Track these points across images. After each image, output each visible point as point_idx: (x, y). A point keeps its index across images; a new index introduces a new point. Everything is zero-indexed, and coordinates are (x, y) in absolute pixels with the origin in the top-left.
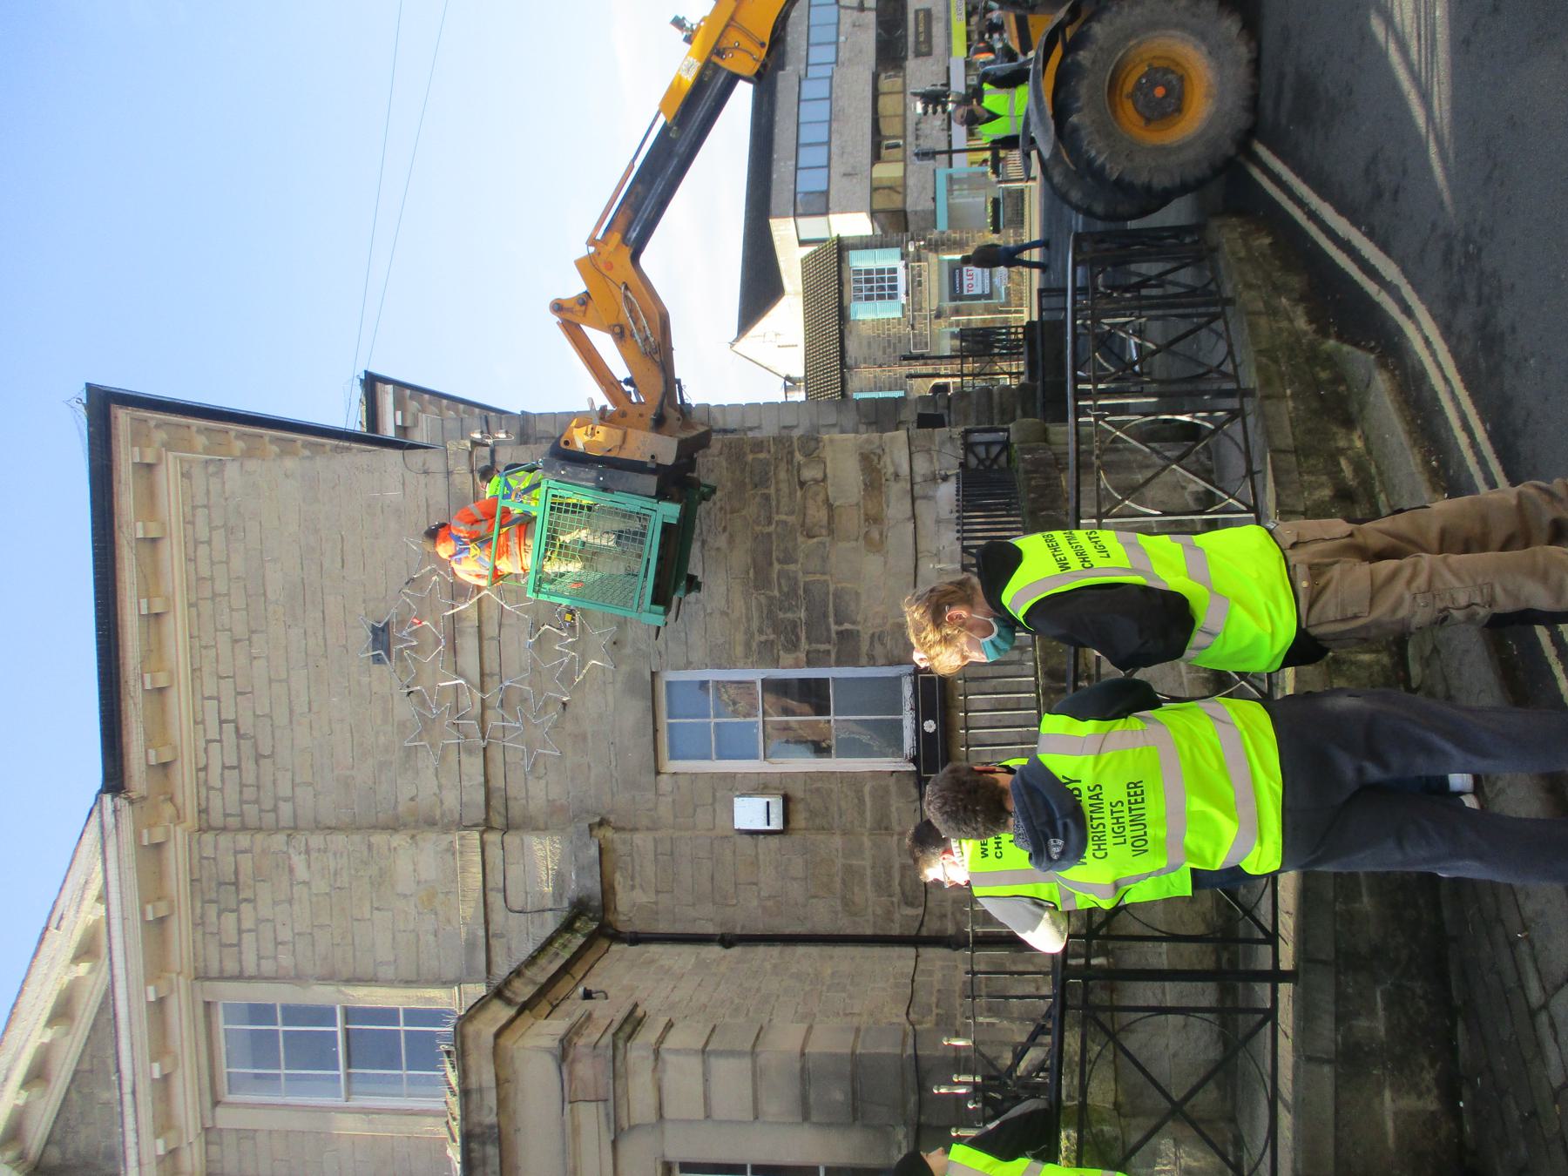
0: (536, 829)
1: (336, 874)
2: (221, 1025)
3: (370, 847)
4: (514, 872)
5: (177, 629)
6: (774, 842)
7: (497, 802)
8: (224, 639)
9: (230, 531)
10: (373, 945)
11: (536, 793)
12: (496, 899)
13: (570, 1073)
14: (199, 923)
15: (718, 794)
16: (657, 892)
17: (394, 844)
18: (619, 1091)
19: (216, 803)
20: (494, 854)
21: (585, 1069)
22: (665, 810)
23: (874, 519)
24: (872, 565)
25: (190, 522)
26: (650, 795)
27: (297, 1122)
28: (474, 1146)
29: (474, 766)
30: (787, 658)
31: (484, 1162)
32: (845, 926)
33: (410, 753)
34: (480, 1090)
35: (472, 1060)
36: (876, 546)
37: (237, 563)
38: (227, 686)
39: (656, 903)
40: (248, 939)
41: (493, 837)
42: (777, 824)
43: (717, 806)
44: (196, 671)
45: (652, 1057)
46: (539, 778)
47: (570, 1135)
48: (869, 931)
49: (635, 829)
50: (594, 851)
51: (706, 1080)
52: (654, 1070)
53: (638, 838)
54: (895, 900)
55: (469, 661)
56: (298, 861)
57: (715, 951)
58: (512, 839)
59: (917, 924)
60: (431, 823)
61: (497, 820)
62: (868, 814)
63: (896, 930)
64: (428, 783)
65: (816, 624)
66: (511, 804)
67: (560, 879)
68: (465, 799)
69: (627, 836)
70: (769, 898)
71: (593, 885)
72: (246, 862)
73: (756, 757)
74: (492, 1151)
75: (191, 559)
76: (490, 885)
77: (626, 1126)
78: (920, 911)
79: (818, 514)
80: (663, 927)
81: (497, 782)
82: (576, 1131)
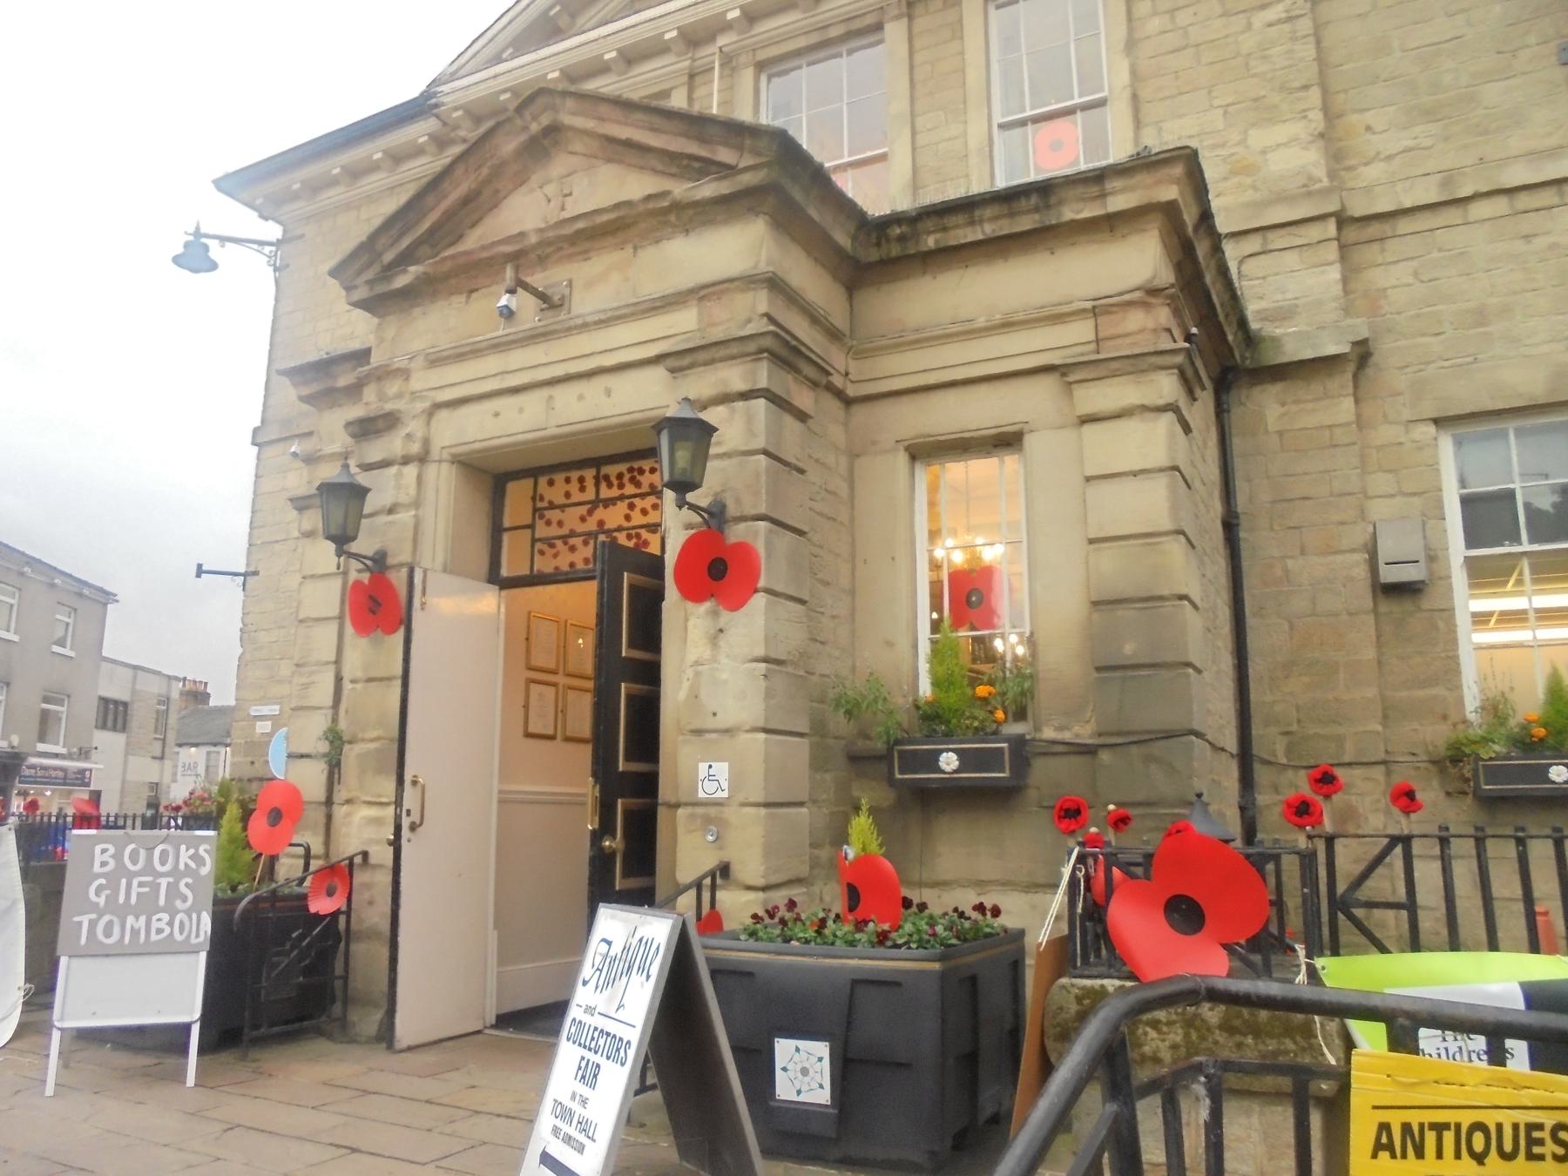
0: (1345, 281)
1: (1265, 57)
3: (1306, 87)
4: (1291, 259)
6: (1361, 572)
7: (1374, 229)
10: (1180, 116)
11: (1395, 273)
12: (1253, 244)
13: (1130, 304)
15: (1415, 500)
16: (1280, 433)
17: (1311, 115)
18: (1115, 365)
20: (1313, 233)
22: (1386, 433)
26: (1407, 414)
27: (974, 77)
28: (1034, 200)
31: (1012, 215)
32: (1255, 667)
34: (1103, 196)
35: (1143, 178)
39: (1267, 432)
41: (1331, 228)
42: (1389, 575)
43: (1398, 500)
45: (1161, 402)
46: (1416, 274)
48: (1254, 696)
49: (1357, 401)
50: (1331, 349)
51: (1135, 474)
52: (1145, 408)
53: (1348, 403)
54: (1295, 727)
57: (1218, 508)
58: (1332, 251)
59: (1265, 756)
60: (1337, 156)
61: (1351, 234)
62: (1405, 694)
63: (1257, 730)
66: (1376, 247)
67: (1284, 314)
68: (1377, 189)
69: (1350, 390)
70: (1286, 571)
71: (1295, 351)
73: (1471, 542)
74: (1025, 223)
76: (1271, 235)
77: (1071, 378)
78: (1284, 761)
80: (1237, 444)
81: (1404, 226)
82: (1057, 319)
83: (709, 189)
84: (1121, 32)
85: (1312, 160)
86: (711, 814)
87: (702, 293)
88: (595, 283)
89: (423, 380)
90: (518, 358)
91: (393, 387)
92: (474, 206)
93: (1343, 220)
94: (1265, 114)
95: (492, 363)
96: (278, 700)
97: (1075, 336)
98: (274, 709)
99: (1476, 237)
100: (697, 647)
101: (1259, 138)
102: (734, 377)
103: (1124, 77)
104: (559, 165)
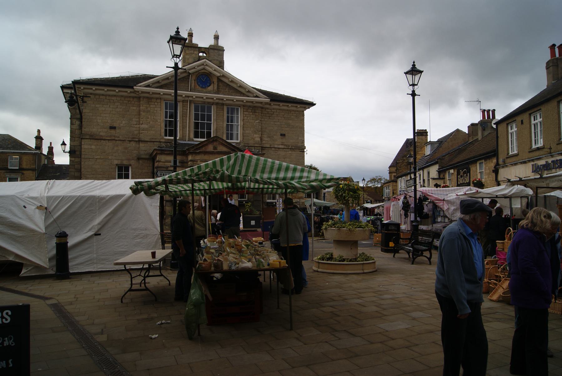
5: (285, 108)
8: (283, 114)
14: (250, 106)
25: (297, 111)
29: (268, 146)
33: (269, 137)
37: (292, 117)
38: (278, 113)
40: (248, 113)
44: (280, 109)
55: (281, 147)
56: (257, 121)
60: (261, 139)
64: (266, 139)
72: (257, 114)
75: (293, 111)
84: (242, 118)
85: (259, 139)
93: (262, 147)
104: (215, 143)
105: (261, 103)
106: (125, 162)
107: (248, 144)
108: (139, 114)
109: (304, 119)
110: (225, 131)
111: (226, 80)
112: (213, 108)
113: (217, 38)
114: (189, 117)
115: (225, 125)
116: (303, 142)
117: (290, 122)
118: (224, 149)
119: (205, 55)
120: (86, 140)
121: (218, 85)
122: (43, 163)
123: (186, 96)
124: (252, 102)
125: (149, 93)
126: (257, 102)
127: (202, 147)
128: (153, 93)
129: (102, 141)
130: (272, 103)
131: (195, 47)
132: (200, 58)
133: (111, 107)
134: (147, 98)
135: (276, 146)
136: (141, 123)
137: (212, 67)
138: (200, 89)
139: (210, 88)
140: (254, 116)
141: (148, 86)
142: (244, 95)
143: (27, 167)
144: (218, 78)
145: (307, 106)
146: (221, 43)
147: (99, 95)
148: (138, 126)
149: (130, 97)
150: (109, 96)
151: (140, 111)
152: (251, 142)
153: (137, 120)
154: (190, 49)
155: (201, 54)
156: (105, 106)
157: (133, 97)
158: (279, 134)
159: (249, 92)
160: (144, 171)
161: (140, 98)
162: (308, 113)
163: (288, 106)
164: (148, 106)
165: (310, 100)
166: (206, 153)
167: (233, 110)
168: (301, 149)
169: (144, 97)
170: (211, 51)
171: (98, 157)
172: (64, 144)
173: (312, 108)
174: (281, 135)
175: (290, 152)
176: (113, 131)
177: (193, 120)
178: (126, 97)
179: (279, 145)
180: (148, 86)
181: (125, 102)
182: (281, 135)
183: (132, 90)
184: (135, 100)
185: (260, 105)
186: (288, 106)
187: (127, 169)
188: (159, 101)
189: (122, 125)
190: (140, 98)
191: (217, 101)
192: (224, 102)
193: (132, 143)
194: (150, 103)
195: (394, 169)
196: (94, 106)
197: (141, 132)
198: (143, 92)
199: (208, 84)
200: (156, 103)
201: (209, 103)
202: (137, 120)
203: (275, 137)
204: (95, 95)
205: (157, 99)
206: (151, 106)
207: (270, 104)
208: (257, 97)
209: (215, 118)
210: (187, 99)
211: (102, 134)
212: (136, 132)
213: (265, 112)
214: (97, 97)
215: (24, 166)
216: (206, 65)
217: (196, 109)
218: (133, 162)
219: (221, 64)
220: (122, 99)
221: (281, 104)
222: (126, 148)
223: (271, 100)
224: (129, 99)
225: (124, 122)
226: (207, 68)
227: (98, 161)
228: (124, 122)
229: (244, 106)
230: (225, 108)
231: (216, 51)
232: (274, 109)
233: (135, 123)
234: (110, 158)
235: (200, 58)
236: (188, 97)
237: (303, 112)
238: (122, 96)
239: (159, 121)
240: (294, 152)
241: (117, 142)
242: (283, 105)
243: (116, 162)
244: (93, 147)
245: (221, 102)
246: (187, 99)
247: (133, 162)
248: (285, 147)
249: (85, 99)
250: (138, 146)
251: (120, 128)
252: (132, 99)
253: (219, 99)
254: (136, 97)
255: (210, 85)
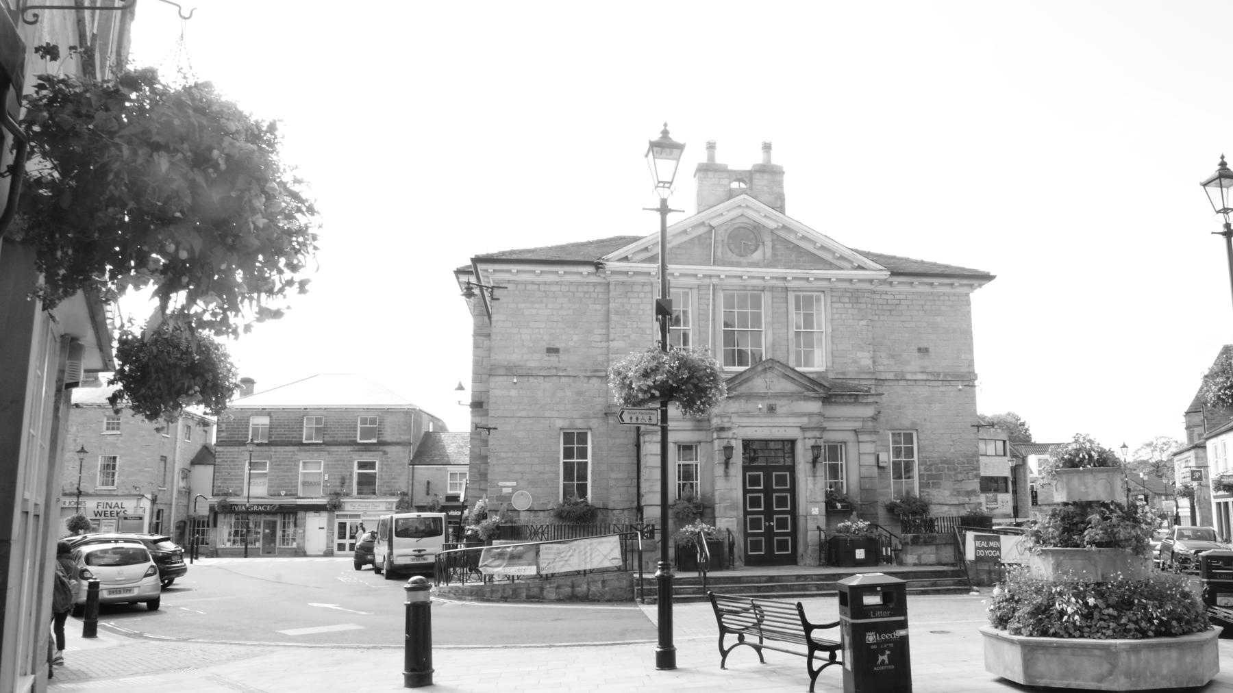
2: (815, 294)
5: (926, 289)
8: (922, 302)
9: (952, 306)
14: (846, 291)
19: (877, 296)
21: (870, 424)
23: (959, 493)
24: (947, 493)
25: (954, 294)
29: (891, 376)
30: (922, 468)
33: (892, 356)
36: (951, 495)
47: (855, 419)
56: (864, 322)
60: (874, 362)
64: (886, 362)
65: (930, 477)
72: (863, 306)
75: (944, 294)
79: (960, 477)
83: (812, 394)
84: (829, 317)
85: (870, 362)
86: (815, 518)
87: (810, 415)
88: (783, 406)
89: (735, 419)
90: (764, 420)
91: (726, 420)
92: (747, 380)
94: (862, 349)
95: (757, 420)
96: (516, 480)
97: (858, 425)
98: (514, 484)
99: (899, 388)
100: (810, 486)
101: (860, 354)
102: (817, 434)
103: (830, 330)
104: (769, 375)
105: (871, 281)
106: (579, 424)
107: (843, 373)
108: (608, 321)
109: (969, 312)
110: (793, 348)
111: (792, 238)
112: (766, 298)
113: (767, 147)
114: (714, 320)
115: (792, 334)
116: (971, 363)
117: (938, 319)
118: (790, 387)
119: (743, 185)
120: (498, 379)
121: (773, 247)
122: (424, 430)
123: (705, 276)
124: (851, 281)
125: (626, 273)
126: (860, 281)
127: (740, 384)
128: (636, 273)
129: (531, 379)
130: (896, 279)
131: (720, 170)
132: (731, 195)
133: (550, 306)
134: (623, 283)
135: (909, 377)
136: (611, 337)
137: (759, 212)
138: (735, 258)
139: (757, 256)
140: (855, 311)
141: (626, 259)
142: (831, 266)
143: (394, 440)
144: (772, 231)
145: (976, 283)
146: (775, 160)
147: (525, 283)
148: (604, 344)
149: (588, 284)
150: (545, 283)
151: (608, 312)
152: (851, 371)
153: (604, 331)
154: (710, 174)
155: (735, 185)
156: (536, 306)
157: (594, 285)
158: (914, 348)
159: (842, 258)
160: (618, 441)
161: (608, 284)
162: (979, 297)
163: (932, 284)
164: (625, 300)
165: (982, 268)
166: (750, 397)
167: (809, 302)
168: (967, 379)
169: (617, 284)
170: (757, 176)
171: (524, 414)
172: (461, 388)
173: (988, 286)
174: (920, 350)
175: (941, 389)
176: (553, 358)
177: (721, 328)
178: (579, 284)
179: (915, 373)
180: (626, 259)
181: (577, 294)
182: (920, 350)
183: (591, 269)
184: (599, 289)
185: (867, 286)
186: (932, 284)
187: (582, 438)
188: (647, 289)
189: (571, 343)
190: (608, 284)
191: (773, 282)
192: (788, 285)
193: (594, 381)
194: (630, 295)
195: (1197, 418)
196: (514, 306)
197: (611, 356)
198: (613, 273)
199: (752, 248)
200: (642, 295)
201: (754, 288)
202: (604, 331)
203: (905, 355)
204: (516, 283)
205: (643, 285)
206: (633, 301)
207: (891, 283)
208: (860, 268)
209: (769, 319)
210: (707, 281)
211: (532, 364)
212: (601, 358)
213: (880, 302)
214: (521, 287)
215: (388, 437)
216: (747, 206)
217: (729, 303)
218: (594, 423)
219: (778, 204)
220: (573, 288)
221: (916, 281)
222: (579, 393)
223: (893, 274)
224: (585, 289)
225: (575, 338)
226: (749, 213)
227: (523, 421)
228: (575, 338)
229: (832, 290)
230: (791, 296)
231: (766, 176)
232: (900, 293)
233: (599, 338)
234: (547, 414)
235: (731, 195)
236: (710, 276)
237: (967, 295)
238: (572, 283)
239: (648, 331)
240: (950, 388)
241: (563, 380)
242: (921, 284)
243: (560, 423)
244: (513, 393)
245: (780, 283)
246: (707, 281)
247: (594, 423)
248: (930, 377)
249: (497, 293)
250: (604, 386)
251: (567, 351)
252: (591, 289)
253: (777, 278)
254: (600, 284)
255: (756, 249)
